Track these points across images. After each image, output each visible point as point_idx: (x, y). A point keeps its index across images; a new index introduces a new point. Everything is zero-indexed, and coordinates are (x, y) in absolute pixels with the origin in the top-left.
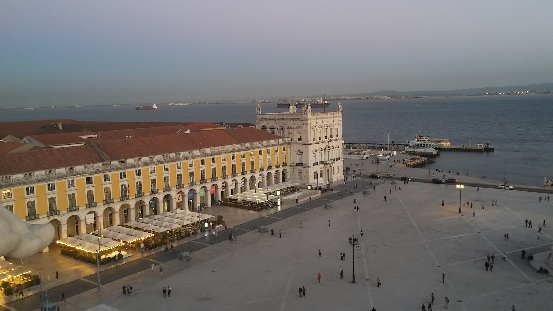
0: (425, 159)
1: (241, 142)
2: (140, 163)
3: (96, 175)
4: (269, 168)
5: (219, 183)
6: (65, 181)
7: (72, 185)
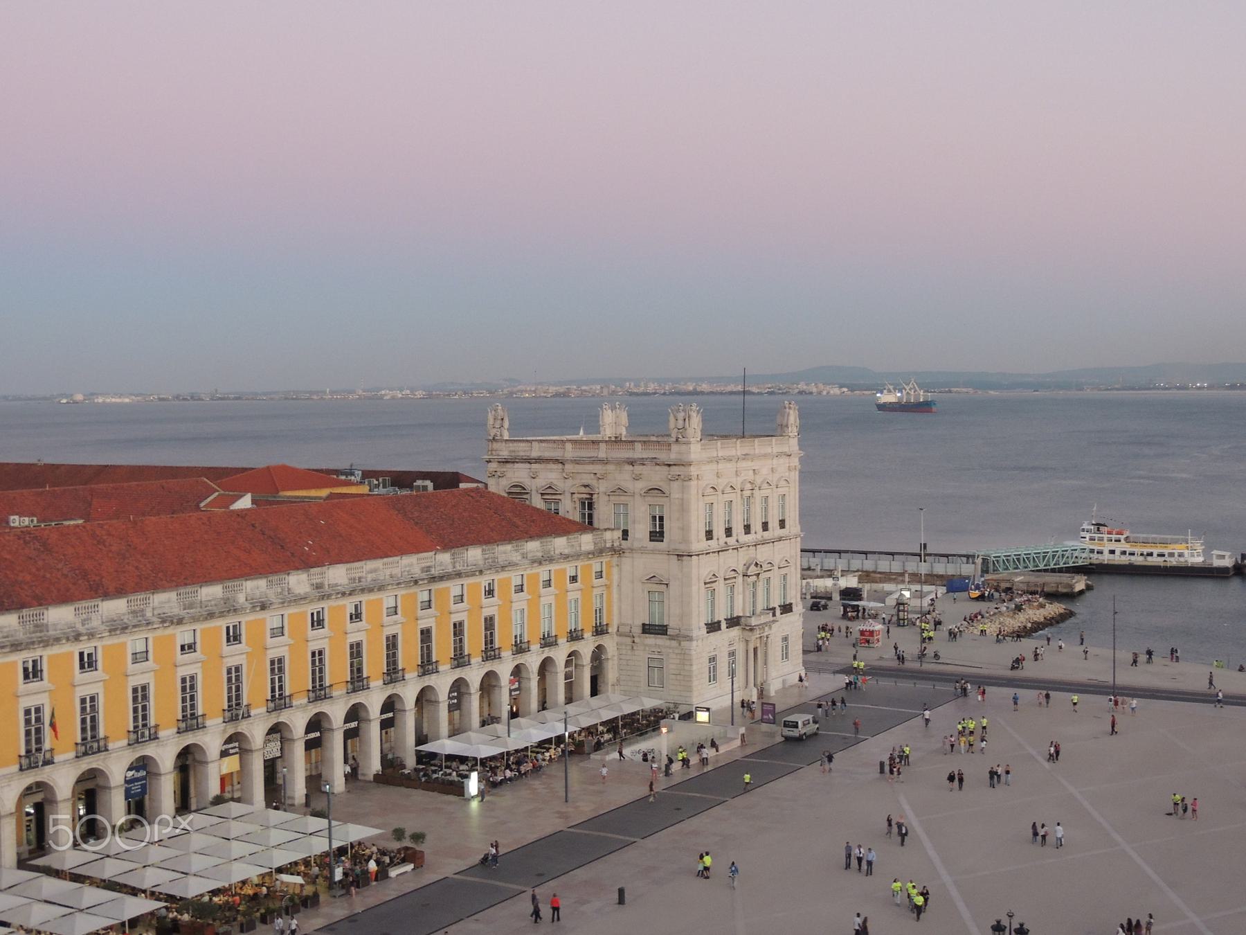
2: (95, 623)
4: (548, 642)
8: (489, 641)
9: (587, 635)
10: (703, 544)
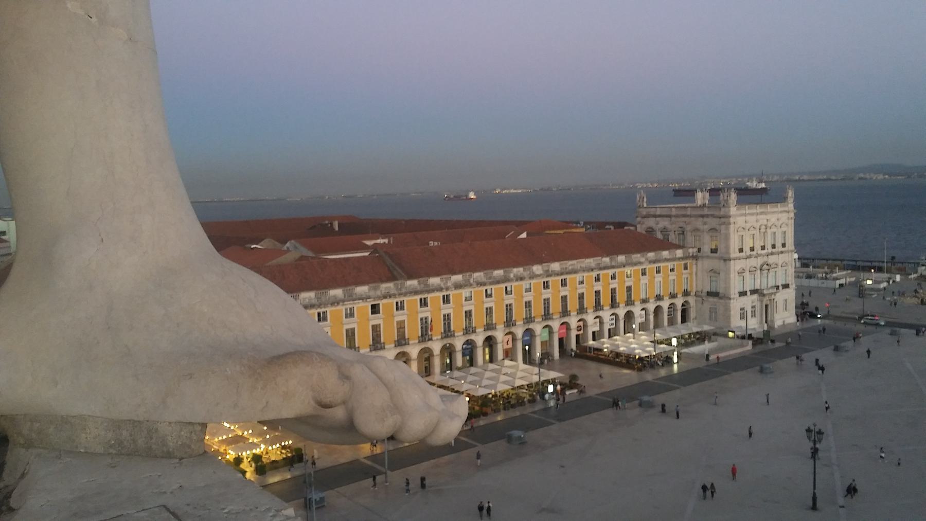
2: (449, 284)
3: (385, 301)
4: (659, 298)
5: (573, 321)
6: (342, 308)
7: (350, 314)
8: (629, 296)
10: (738, 254)
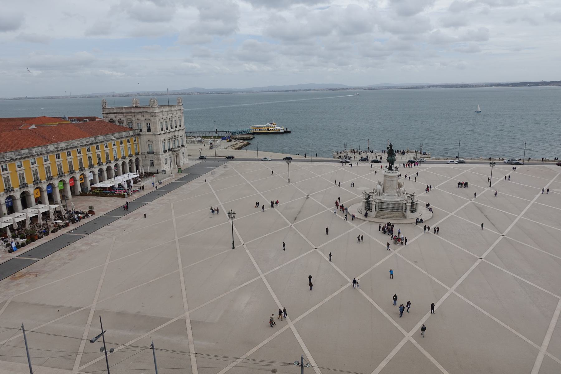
0: (245, 142)
1: (95, 135)
4: (123, 158)
5: (78, 176)
8: (108, 158)
9: (134, 155)
10: (160, 132)
